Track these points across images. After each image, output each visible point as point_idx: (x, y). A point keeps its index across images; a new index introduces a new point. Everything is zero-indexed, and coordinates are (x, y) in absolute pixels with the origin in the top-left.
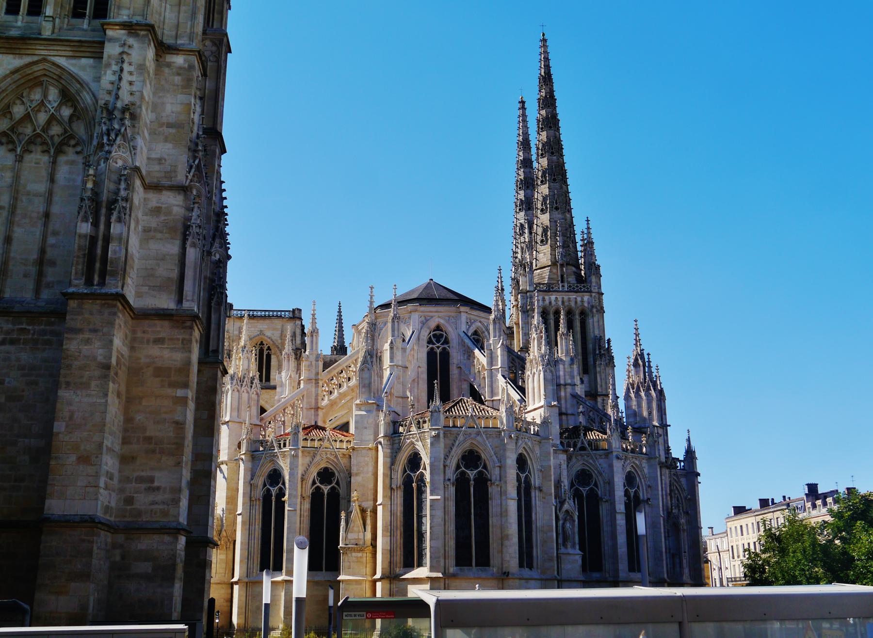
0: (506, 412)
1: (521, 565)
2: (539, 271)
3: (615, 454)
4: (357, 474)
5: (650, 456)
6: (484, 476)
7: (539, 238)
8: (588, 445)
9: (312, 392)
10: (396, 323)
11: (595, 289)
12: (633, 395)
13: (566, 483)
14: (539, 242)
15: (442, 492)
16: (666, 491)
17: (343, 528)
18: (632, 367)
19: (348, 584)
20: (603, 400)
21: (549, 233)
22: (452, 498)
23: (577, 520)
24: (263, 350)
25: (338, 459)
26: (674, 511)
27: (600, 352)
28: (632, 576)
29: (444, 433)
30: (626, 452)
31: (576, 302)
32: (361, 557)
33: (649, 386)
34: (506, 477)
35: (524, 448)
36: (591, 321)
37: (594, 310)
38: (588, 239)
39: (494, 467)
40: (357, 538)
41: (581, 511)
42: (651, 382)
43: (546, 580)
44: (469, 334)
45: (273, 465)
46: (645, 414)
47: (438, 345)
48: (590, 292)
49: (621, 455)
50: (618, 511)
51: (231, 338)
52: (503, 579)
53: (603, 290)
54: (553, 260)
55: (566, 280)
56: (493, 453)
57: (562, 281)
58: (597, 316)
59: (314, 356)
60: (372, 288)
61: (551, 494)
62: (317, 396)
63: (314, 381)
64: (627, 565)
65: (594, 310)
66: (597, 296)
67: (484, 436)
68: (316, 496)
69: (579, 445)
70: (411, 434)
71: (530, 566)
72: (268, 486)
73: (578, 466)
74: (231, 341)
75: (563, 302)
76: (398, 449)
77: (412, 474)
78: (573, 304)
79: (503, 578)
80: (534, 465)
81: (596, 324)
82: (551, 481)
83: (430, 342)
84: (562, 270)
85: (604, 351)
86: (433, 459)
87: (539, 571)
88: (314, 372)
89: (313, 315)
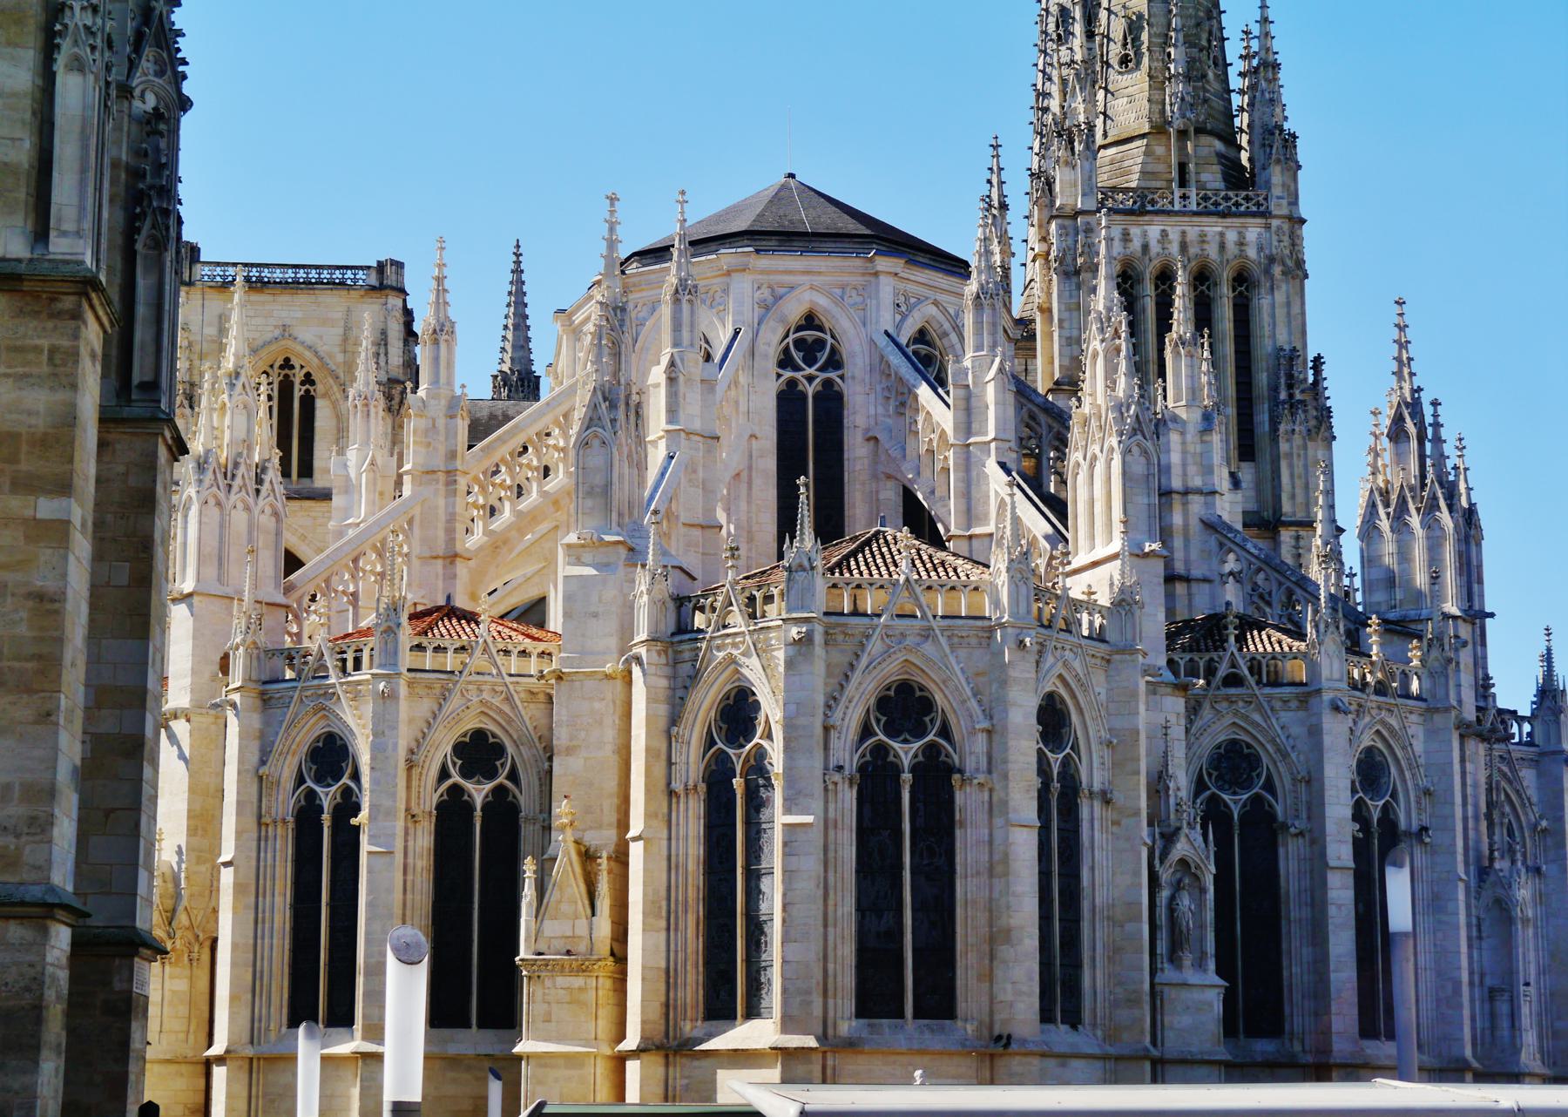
0: (1008, 570)
1: (1046, 1016)
2: (1113, 150)
3: (1327, 697)
4: (570, 751)
5: (1431, 706)
6: (942, 758)
7: (1115, 51)
8: (1251, 669)
10: (685, 306)
11: (1279, 207)
12: (1384, 524)
13: (1181, 782)
14: (1114, 61)
15: (818, 805)
16: (1476, 806)
17: (530, 904)
18: (1385, 442)
19: (545, 1066)
20: (1298, 538)
21: (1145, 36)
22: (847, 821)
23: (1211, 889)
24: (292, 384)
25: (514, 707)
26: (1497, 865)
27: (1291, 396)
28: (1369, 1051)
29: (826, 633)
30: (1363, 690)
31: (1222, 246)
32: (580, 989)
33: (1434, 498)
34: (1005, 761)
35: (1060, 676)
36: (1265, 302)
37: (1277, 270)
38: (1263, 54)
39: (973, 732)
40: (569, 933)
41: (1223, 862)
42: (1441, 485)
43: (1118, 1058)
44: (903, 341)
45: (323, 723)
46: (1421, 579)
48: (1266, 214)
49: (1346, 700)
50: (1332, 863)
51: (197, 348)
52: (992, 1056)
53: (1304, 211)
54: (1156, 117)
55: (1192, 177)
56: (969, 693)
57: (1183, 183)
58: (1284, 287)
59: (443, 402)
60: (613, 200)
61: (1137, 813)
62: (451, 519)
63: (442, 477)
64: (1356, 1017)
66: (1286, 227)
67: (943, 641)
68: (452, 812)
69: (1223, 670)
70: (728, 635)
71: (1073, 1019)
72: (310, 783)
73: (1218, 729)
74: (195, 357)
75: (1184, 247)
76: (690, 677)
77: (731, 751)
78: (1212, 251)
79: (991, 1050)
80: (1087, 727)
81: (1280, 313)
82: (1138, 773)
83: (785, 362)
84: (1182, 149)
85: (1303, 391)
86: (793, 707)
87: (1099, 1033)
88: (442, 450)
89: (440, 280)
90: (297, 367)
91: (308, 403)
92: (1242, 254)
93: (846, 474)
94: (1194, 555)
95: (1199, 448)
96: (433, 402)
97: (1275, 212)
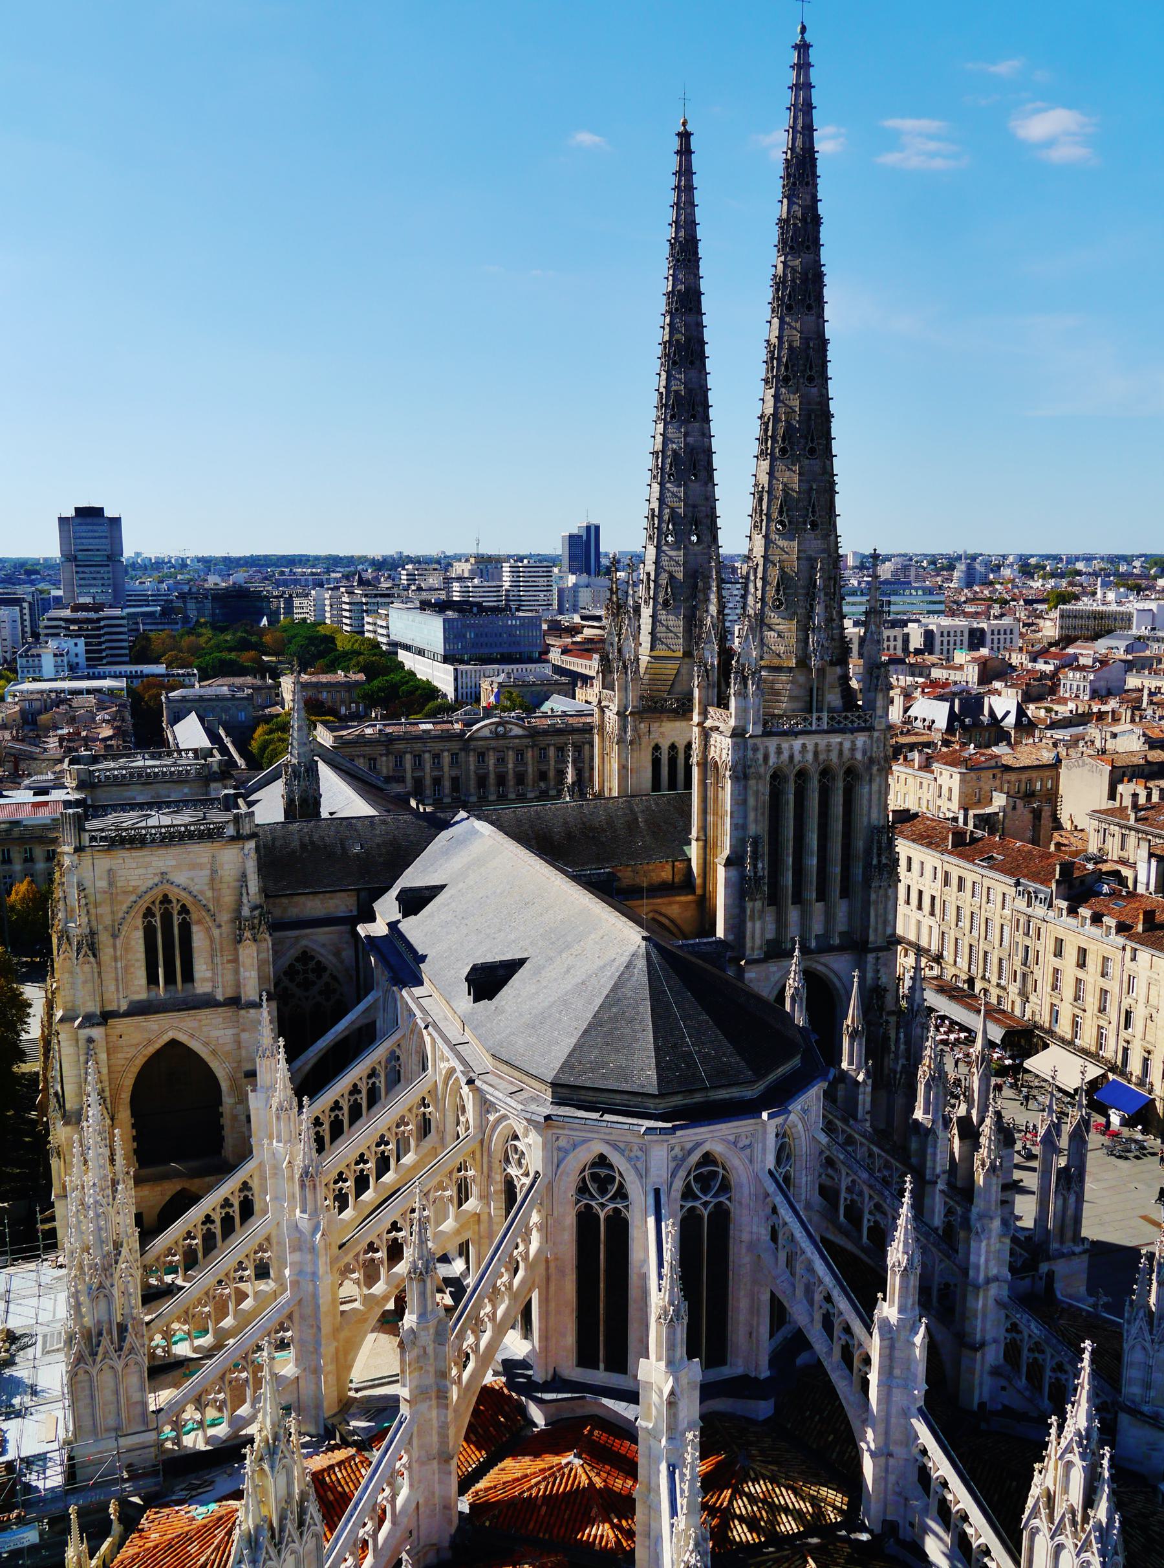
9: (430, 1420)
20: (878, 958)
24: (171, 915)
27: (879, 861)
31: (841, 753)
36: (866, 790)
37: (875, 768)
47: (706, 1199)
48: (871, 729)
51: (92, 899)
58: (878, 779)
59: (432, 1331)
65: (875, 768)
74: (91, 906)
75: (816, 754)
81: (875, 797)
88: (432, 1370)
90: (175, 901)
91: (186, 928)
92: (853, 758)
93: (731, 1273)
94: (988, 1327)
95: (998, 1246)
96: (422, 1333)
97: (877, 728)
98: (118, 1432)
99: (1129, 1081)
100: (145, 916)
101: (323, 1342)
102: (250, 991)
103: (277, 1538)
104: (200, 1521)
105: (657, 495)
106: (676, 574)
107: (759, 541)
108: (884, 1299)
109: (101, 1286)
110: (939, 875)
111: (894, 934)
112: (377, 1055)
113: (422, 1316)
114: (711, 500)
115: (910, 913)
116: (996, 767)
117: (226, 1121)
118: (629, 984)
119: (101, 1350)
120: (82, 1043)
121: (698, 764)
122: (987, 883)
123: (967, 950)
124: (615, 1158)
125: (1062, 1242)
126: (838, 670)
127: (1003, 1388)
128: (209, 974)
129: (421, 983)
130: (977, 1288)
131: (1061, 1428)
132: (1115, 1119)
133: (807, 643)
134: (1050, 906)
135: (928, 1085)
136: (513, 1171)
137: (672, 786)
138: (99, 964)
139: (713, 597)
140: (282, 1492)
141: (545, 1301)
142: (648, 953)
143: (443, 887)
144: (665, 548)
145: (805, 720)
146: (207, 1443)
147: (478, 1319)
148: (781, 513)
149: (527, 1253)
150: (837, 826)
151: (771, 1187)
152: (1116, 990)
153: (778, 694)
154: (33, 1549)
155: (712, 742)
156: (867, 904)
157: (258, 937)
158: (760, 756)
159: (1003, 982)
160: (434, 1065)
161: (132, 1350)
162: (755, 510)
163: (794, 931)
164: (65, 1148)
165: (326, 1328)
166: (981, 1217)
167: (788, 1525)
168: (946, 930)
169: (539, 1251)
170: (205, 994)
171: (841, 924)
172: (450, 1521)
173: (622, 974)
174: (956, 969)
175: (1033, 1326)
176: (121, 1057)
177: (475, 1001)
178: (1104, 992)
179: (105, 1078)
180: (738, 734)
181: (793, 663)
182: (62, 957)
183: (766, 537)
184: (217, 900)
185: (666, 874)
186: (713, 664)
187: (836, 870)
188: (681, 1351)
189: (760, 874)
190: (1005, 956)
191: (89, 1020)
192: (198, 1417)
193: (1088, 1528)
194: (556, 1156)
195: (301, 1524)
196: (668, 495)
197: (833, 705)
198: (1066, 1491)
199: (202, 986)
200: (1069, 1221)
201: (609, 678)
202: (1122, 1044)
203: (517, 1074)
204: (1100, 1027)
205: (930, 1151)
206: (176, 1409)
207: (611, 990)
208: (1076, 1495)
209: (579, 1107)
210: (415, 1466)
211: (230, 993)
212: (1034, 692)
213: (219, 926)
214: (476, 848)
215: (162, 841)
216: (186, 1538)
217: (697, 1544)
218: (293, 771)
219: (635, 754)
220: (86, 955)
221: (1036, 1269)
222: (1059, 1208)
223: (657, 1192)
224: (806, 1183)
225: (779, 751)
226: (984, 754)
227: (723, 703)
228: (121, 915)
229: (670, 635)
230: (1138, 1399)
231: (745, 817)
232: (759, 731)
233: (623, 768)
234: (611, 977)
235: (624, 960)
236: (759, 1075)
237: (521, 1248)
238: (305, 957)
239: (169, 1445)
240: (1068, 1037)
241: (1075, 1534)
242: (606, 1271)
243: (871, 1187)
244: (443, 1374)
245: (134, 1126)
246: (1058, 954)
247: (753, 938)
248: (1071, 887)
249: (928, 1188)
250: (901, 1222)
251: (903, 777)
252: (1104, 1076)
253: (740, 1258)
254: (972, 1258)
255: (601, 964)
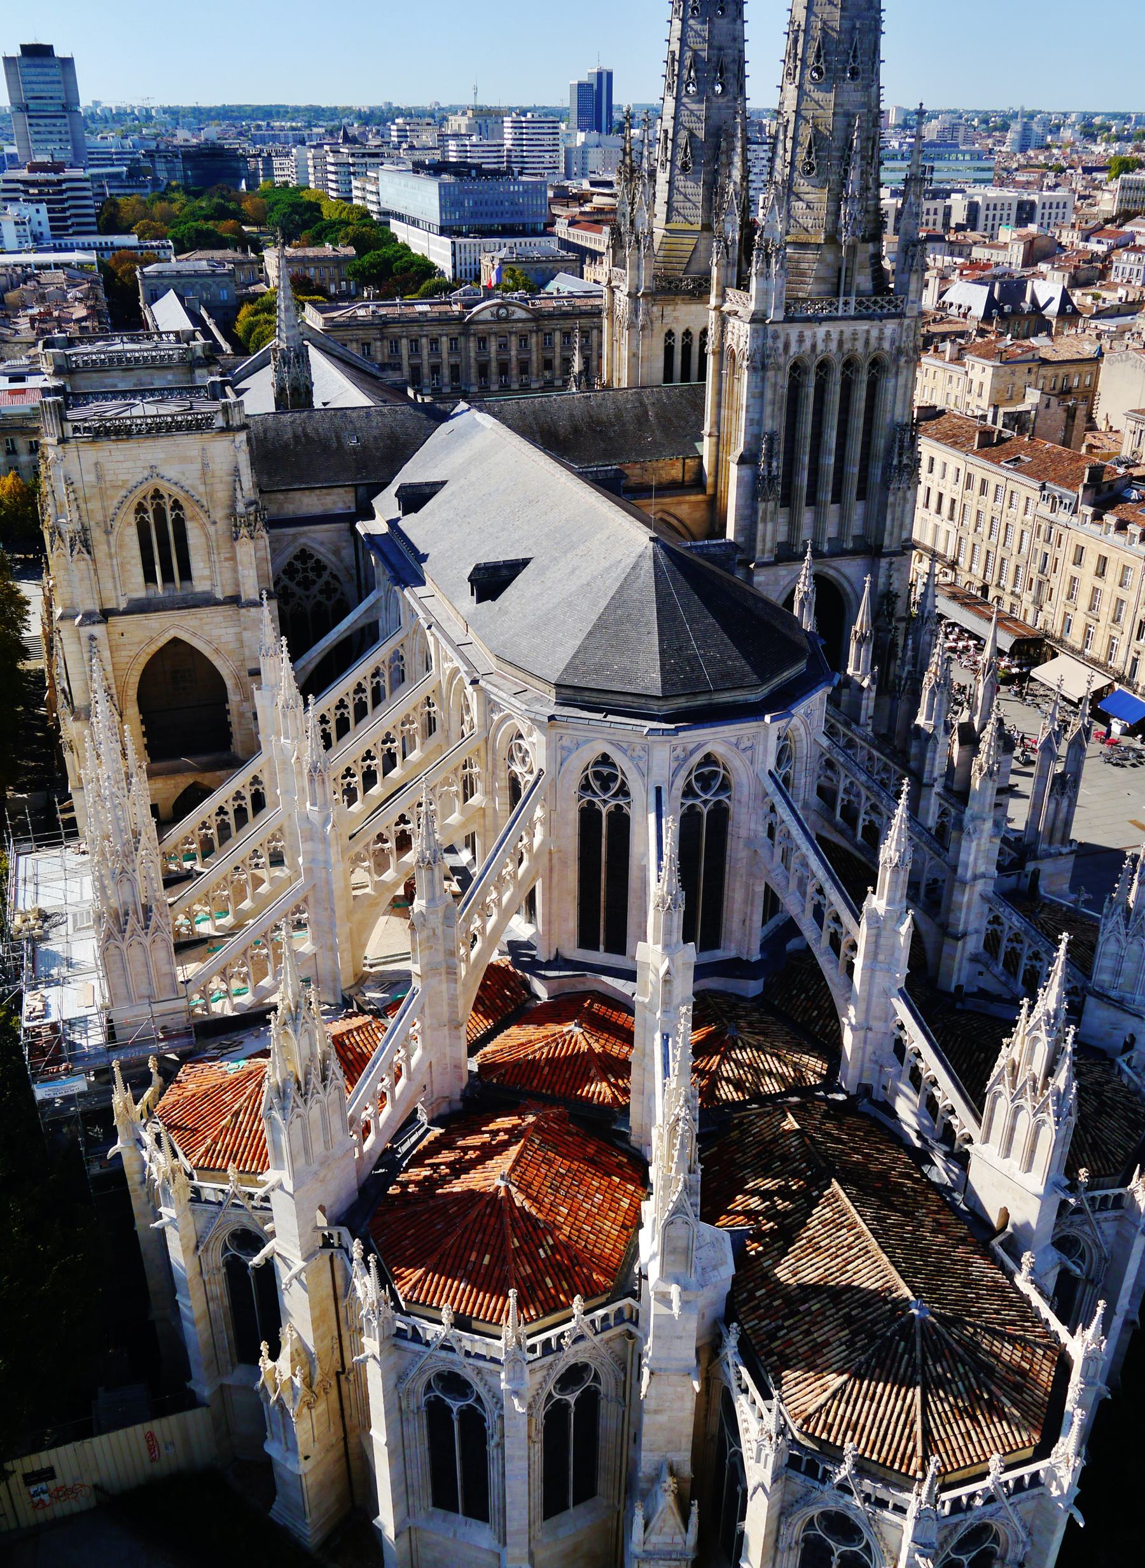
4: (656, 1412)
20: (891, 564)
24: (164, 510)
27: (900, 462)
36: (892, 383)
37: (903, 359)
47: (705, 797)
48: (901, 315)
51: (81, 494)
59: (441, 914)
68: (555, 1416)
74: (80, 501)
75: (841, 343)
81: (900, 392)
88: (441, 948)
91: (180, 524)
92: (880, 348)
94: (972, 917)
98: (151, 1000)
99: (1135, 692)
100: (137, 512)
101: (338, 923)
102: (250, 589)
103: (303, 1089)
104: (232, 1075)
105: (678, 34)
106: (696, 132)
107: (791, 91)
108: (874, 892)
109: (123, 871)
110: (962, 477)
111: (909, 539)
112: (378, 656)
113: (431, 901)
114: (738, 40)
115: (927, 517)
116: (1033, 360)
117: (233, 718)
118: (635, 586)
119: (128, 927)
120: (84, 640)
121: (714, 353)
122: (1011, 486)
123: (984, 557)
124: (617, 757)
125: (1050, 843)
126: (870, 248)
127: (981, 973)
128: (207, 572)
129: (423, 583)
130: (964, 883)
131: (1031, 1008)
132: (1116, 727)
133: (838, 216)
134: (1075, 512)
135: (933, 693)
136: (517, 768)
137: (685, 377)
138: (94, 560)
139: (737, 160)
140: (306, 1052)
141: (548, 889)
142: (655, 555)
143: (444, 483)
144: (685, 100)
145: (831, 304)
146: (234, 1010)
147: (483, 903)
148: (818, 57)
149: (531, 845)
150: (858, 423)
151: (771, 787)
152: (1133, 600)
153: (803, 275)
154: (81, 1095)
155: (730, 328)
156: (883, 506)
157: (255, 534)
158: (780, 345)
159: (1018, 590)
160: (438, 666)
161: (157, 928)
162: (788, 54)
163: (806, 534)
164: (76, 743)
165: (340, 909)
166: (973, 818)
167: (770, 1086)
168: (964, 535)
169: (543, 843)
170: (204, 593)
171: (856, 528)
172: (461, 1078)
173: (629, 575)
174: (970, 576)
175: (1014, 918)
176: (124, 655)
177: (479, 601)
178: (1120, 602)
179: (110, 675)
180: (757, 319)
181: (821, 239)
182: (56, 553)
183: (800, 87)
184: (210, 495)
185: (675, 471)
186: (733, 240)
187: (853, 470)
188: (678, 935)
189: (775, 473)
190: (1022, 563)
191: (89, 618)
192: (224, 987)
193: (1046, 1093)
194: (560, 755)
195: (324, 1078)
196: (692, 34)
197: (862, 288)
198: (1030, 1061)
199: (201, 583)
200: (1060, 824)
201: (620, 254)
202: (1133, 654)
203: (521, 675)
204: (1112, 637)
205: (929, 755)
206: (203, 981)
207: (617, 592)
208: (1039, 1066)
209: (582, 708)
210: (428, 1032)
211: (229, 592)
212: (1082, 276)
213: (215, 523)
214: (478, 442)
215: (148, 432)
216: (220, 1089)
217: (686, 1101)
218: (283, 357)
219: (647, 341)
220: (80, 552)
221: (1023, 868)
222: (1051, 811)
223: (658, 790)
224: (805, 784)
225: (801, 340)
226: (1020, 346)
227: (742, 284)
228: (111, 511)
229: (689, 204)
230: (1107, 985)
231: (762, 412)
232: (781, 316)
233: (634, 355)
234: (616, 579)
235: (631, 561)
236: (764, 680)
237: (525, 840)
238: (304, 555)
239: (199, 1011)
240: (1079, 646)
241: (1034, 1098)
242: (608, 862)
243: (868, 788)
244: (452, 953)
245: (142, 722)
246: (1078, 561)
247: (764, 540)
248: (1098, 492)
249: (925, 791)
250: (895, 822)
251: (932, 370)
252: (1110, 686)
253: (737, 852)
254: (962, 856)
255: (607, 564)
